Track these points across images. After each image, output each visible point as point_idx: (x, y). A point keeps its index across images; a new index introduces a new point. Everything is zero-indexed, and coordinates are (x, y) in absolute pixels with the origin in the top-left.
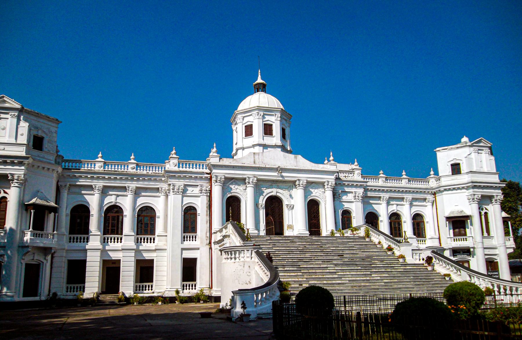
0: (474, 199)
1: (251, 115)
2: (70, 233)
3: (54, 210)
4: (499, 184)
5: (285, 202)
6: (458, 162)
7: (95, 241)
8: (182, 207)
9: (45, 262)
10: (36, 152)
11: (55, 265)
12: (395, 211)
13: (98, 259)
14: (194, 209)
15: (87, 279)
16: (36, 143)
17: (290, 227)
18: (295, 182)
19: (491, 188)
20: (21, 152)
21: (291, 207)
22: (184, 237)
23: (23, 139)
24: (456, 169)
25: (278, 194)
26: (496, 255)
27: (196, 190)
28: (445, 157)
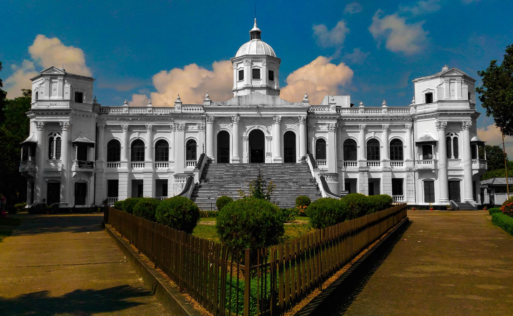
0: (440, 126)
1: (242, 62)
2: (108, 161)
3: (92, 145)
4: (470, 111)
5: (266, 135)
6: (431, 91)
7: (123, 166)
8: (185, 141)
9: (89, 181)
10: (78, 105)
11: (97, 183)
12: (373, 137)
13: (127, 179)
14: (195, 142)
15: (119, 194)
16: (78, 97)
17: (270, 154)
18: (272, 118)
19: (459, 115)
20: (65, 106)
21: (271, 139)
22: (187, 163)
23: (68, 97)
24: (429, 98)
25: (259, 128)
26: (461, 176)
27: (196, 128)
28: (421, 87)
